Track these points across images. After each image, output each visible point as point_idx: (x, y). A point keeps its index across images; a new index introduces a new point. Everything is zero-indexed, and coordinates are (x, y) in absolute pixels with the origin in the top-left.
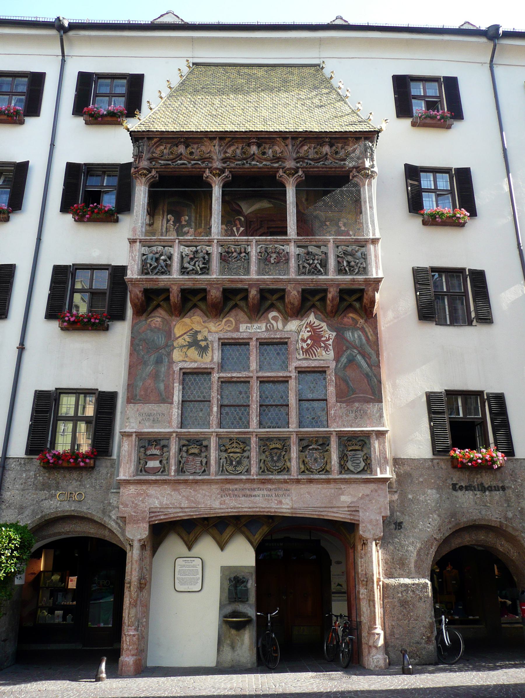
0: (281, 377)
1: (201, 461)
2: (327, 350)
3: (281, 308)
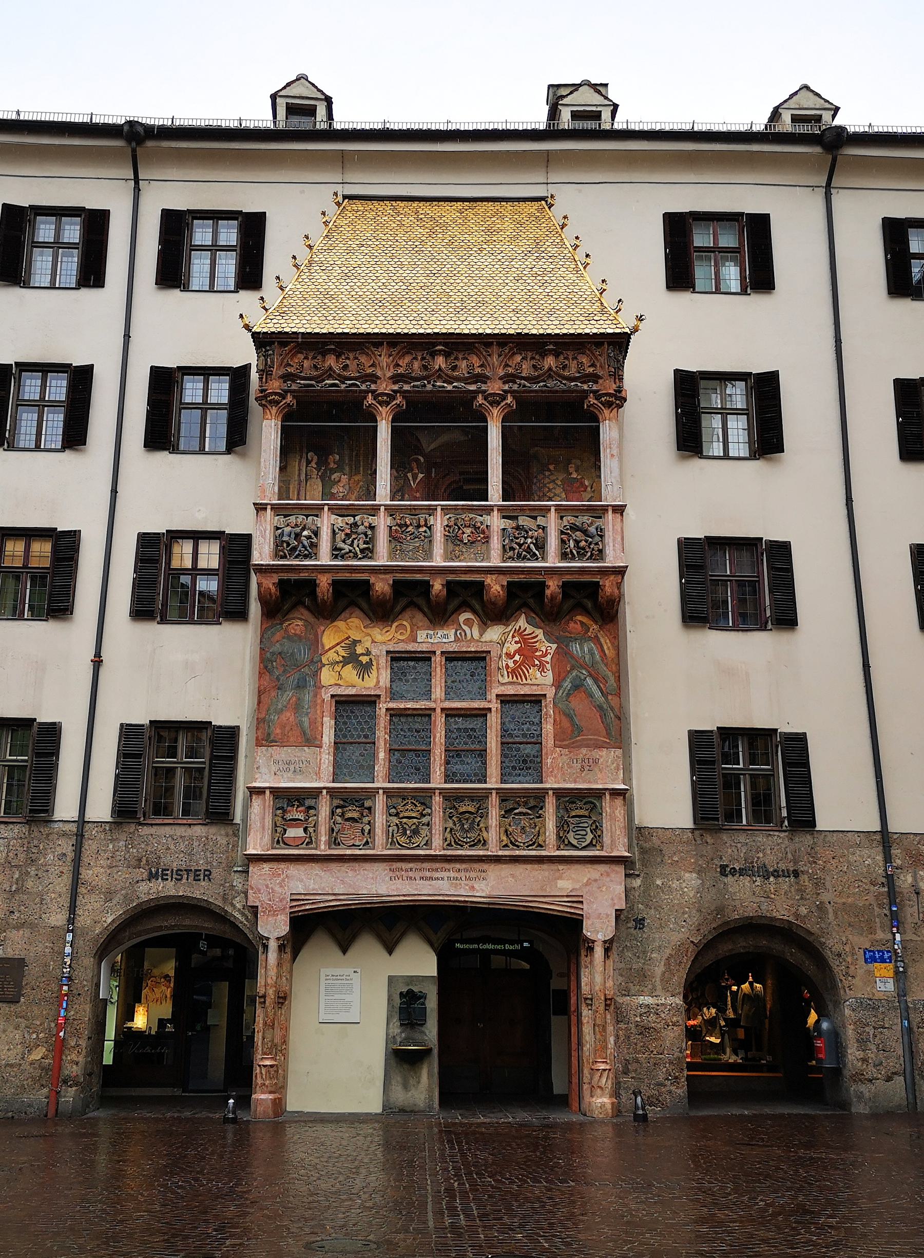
0: (476, 709)
1: (363, 830)
2: (543, 670)
3: (477, 607)
